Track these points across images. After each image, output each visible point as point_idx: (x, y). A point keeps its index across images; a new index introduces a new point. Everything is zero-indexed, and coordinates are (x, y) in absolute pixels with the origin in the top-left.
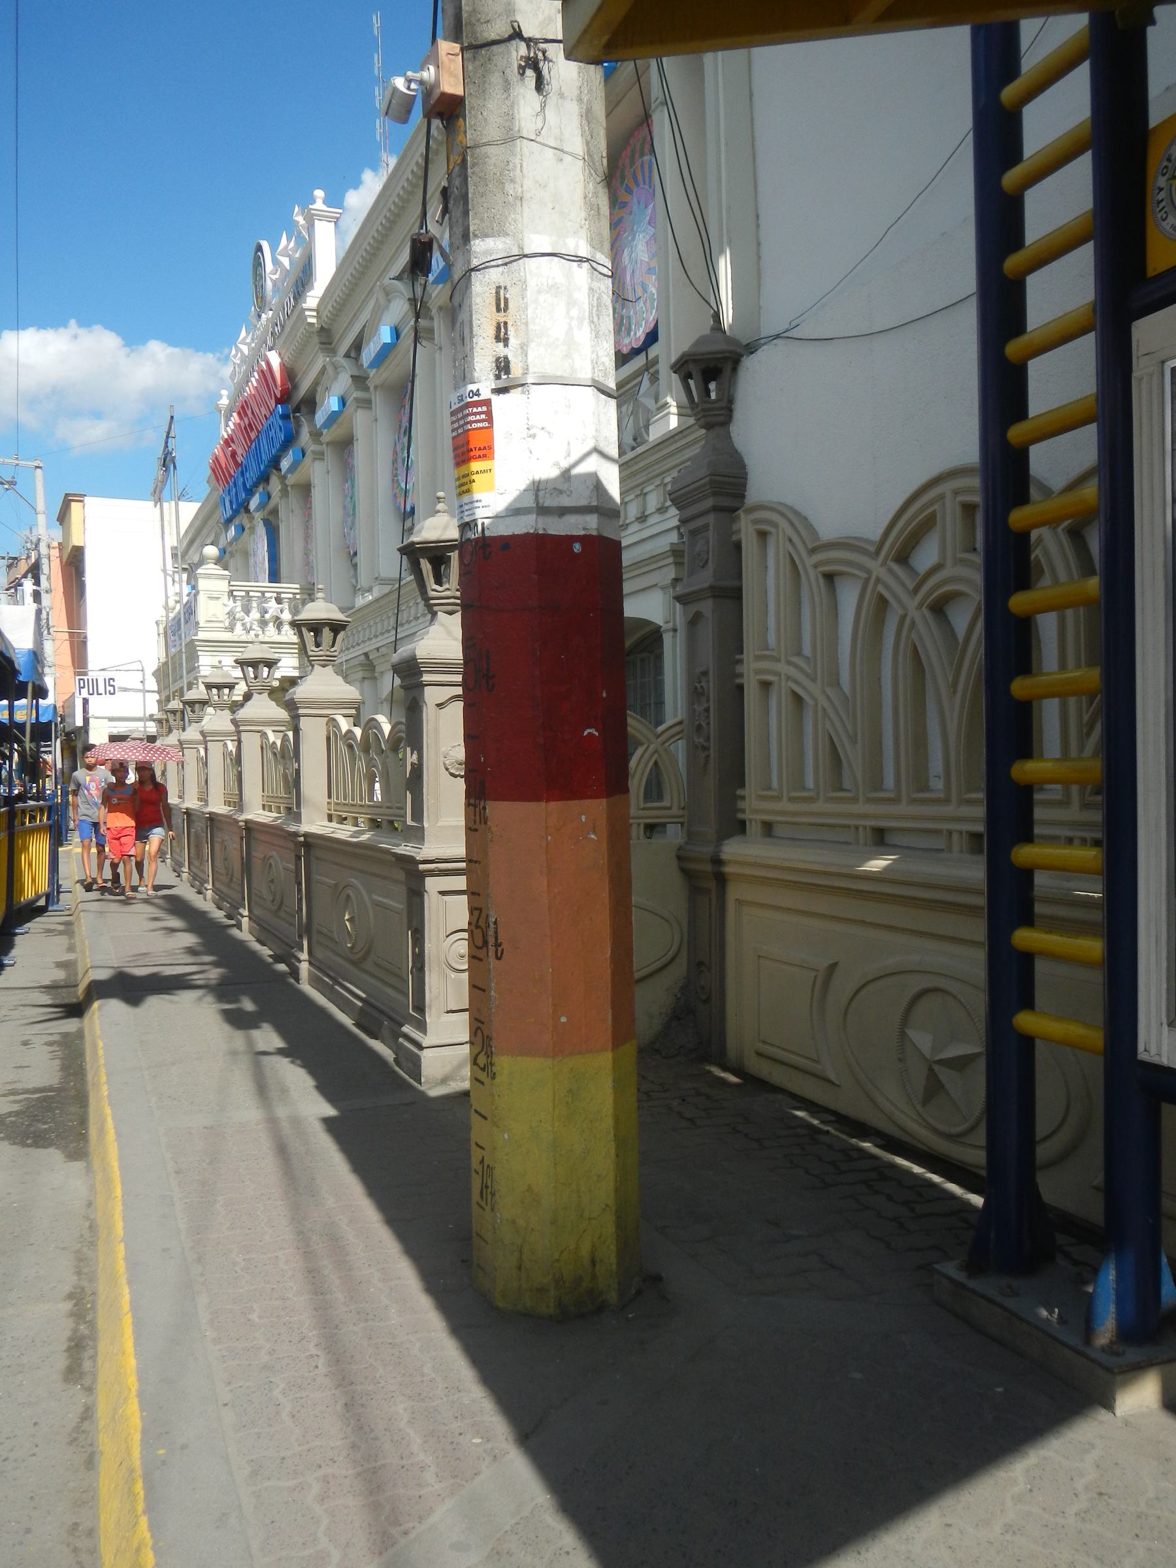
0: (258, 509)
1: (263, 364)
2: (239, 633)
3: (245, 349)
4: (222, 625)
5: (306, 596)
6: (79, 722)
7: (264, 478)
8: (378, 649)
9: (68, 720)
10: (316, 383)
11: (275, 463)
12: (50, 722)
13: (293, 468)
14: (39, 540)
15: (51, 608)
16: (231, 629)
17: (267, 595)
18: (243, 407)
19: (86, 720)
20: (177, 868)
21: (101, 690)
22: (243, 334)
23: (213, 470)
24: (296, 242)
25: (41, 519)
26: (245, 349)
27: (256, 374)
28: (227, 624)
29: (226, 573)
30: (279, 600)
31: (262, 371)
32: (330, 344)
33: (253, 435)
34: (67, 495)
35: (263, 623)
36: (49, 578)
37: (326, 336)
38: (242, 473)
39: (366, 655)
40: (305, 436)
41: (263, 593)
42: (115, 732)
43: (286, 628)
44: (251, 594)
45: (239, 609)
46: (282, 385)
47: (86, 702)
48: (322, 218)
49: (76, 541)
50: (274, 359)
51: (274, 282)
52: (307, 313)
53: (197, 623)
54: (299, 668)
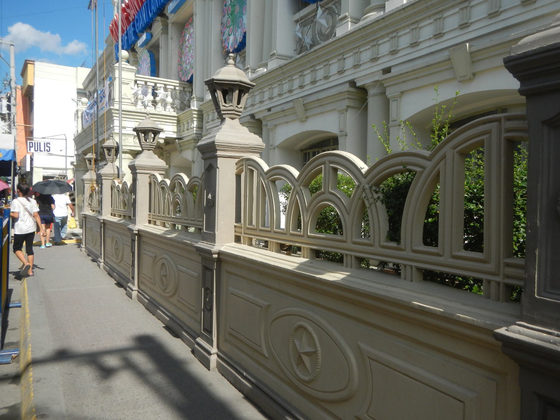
0: (142, 46)
2: (140, 107)
4: (129, 101)
5: (182, 89)
6: (28, 169)
7: (148, 26)
8: (269, 110)
9: (22, 169)
11: (161, 12)
12: (10, 161)
13: (174, 11)
14: (11, 79)
15: (16, 114)
16: (135, 104)
17: (158, 85)
19: (32, 168)
20: (122, 282)
21: (42, 149)
23: (112, 31)
25: (13, 70)
28: (133, 100)
29: (134, 68)
30: (166, 89)
34: (26, 60)
35: (154, 103)
36: (15, 99)
38: (134, 26)
41: (156, 84)
42: (46, 174)
43: (169, 107)
45: (140, 92)
47: (32, 160)
49: (30, 83)
54: (177, 132)
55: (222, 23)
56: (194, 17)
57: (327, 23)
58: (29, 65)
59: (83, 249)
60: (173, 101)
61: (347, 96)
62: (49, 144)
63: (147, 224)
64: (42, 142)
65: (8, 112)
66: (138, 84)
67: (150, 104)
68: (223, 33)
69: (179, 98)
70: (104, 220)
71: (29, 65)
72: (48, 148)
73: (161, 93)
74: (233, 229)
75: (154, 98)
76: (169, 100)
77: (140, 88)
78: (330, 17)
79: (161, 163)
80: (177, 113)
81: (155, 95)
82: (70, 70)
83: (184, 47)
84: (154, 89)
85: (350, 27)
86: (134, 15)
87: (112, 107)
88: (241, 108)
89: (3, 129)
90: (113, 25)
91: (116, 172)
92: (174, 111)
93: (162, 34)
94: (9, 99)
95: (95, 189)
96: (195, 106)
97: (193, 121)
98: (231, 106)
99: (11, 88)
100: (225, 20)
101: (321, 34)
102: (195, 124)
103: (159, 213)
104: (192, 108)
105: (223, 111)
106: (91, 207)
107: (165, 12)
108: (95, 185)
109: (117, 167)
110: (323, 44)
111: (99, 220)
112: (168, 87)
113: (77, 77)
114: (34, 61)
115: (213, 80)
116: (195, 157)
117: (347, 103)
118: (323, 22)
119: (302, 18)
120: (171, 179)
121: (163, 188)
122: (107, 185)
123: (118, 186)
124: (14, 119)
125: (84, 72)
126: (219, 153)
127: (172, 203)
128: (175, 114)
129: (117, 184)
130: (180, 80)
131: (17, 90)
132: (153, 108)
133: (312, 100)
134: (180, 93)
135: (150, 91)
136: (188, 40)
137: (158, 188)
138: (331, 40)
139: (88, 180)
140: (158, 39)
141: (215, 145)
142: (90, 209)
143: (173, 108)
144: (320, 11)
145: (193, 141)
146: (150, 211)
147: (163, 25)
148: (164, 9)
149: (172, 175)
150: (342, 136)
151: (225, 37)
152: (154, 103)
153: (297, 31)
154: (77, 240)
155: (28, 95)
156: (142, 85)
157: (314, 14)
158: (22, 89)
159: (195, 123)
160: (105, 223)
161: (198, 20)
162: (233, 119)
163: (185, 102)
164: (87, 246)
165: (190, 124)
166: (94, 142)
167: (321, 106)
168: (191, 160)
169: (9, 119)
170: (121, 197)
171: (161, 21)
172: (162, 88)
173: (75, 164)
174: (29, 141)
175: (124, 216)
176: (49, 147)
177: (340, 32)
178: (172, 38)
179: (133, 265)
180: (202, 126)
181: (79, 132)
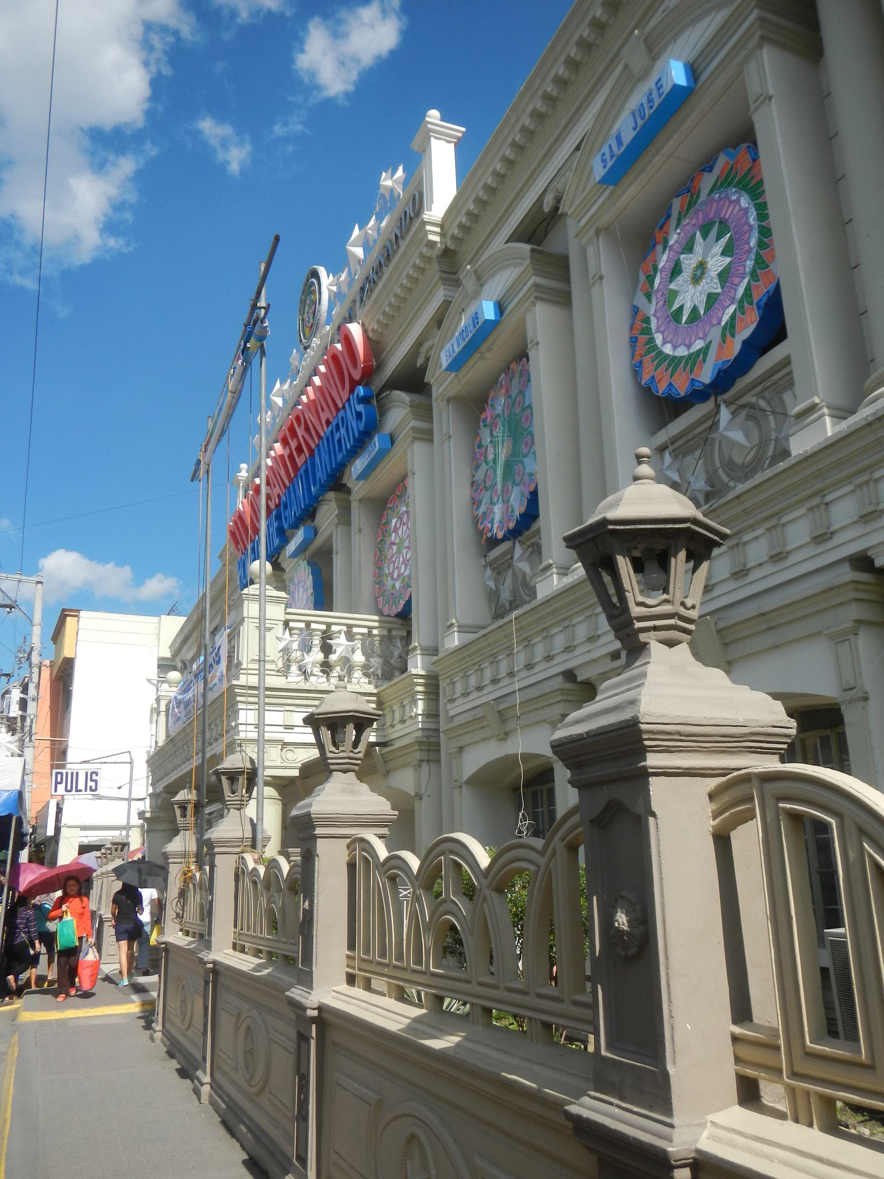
0: (294, 555)
1: (339, 346)
2: (294, 679)
3: (279, 401)
5: (386, 633)
6: (50, 832)
7: (309, 514)
9: (39, 831)
10: (419, 344)
11: (336, 483)
12: (10, 816)
13: (364, 475)
14: (32, 648)
16: (285, 672)
17: (334, 628)
18: (292, 430)
19: (58, 830)
21: (81, 786)
22: (278, 386)
23: (233, 534)
24: (377, 219)
25: (37, 630)
26: (279, 401)
27: (322, 368)
28: (280, 665)
29: (282, 594)
30: (350, 636)
31: (335, 357)
32: (455, 273)
33: (300, 461)
37: (449, 260)
39: (569, 675)
40: (399, 411)
41: (329, 625)
42: (86, 841)
43: (357, 674)
44: (313, 626)
45: (295, 646)
46: (364, 362)
47: (59, 811)
48: (441, 136)
49: (67, 653)
50: (355, 330)
51: (335, 298)
52: (428, 228)
53: (239, 664)
55: (473, 483)
56: (409, 481)
57: (748, 436)
58: (68, 618)
59: (158, 1035)
60: (367, 660)
61: (853, 595)
62: (97, 774)
63: (344, 987)
64: (82, 770)
65: (21, 713)
66: (291, 629)
67: (317, 670)
68: (476, 503)
69: (378, 652)
70: (214, 963)
71: (68, 618)
72: (93, 784)
73: (340, 643)
74: (727, 1050)
75: (326, 657)
76: (359, 658)
77: (295, 637)
78: (751, 424)
79: (380, 805)
80: (376, 687)
81: (327, 649)
82: (145, 624)
83: (386, 546)
84: (327, 636)
85: (830, 428)
86: (279, 496)
87: (234, 682)
88: (693, 607)
89: (8, 749)
90: (235, 522)
91: (248, 834)
92: (370, 683)
93: (337, 525)
94: (25, 689)
95: (193, 878)
96: (417, 666)
97: (414, 702)
98: (667, 601)
99: (30, 664)
100: (480, 475)
101: (730, 466)
102: (420, 707)
103: (383, 954)
104: (414, 671)
105: (641, 619)
106: (181, 923)
107: (345, 480)
108: (193, 867)
109: (251, 820)
110: (741, 488)
111: (202, 962)
112: (355, 630)
113: (159, 635)
114: (78, 611)
115: (604, 522)
116: (423, 784)
117: (854, 612)
118: (738, 436)
119: (674, 440)
120: (423, 853)
121: (393, 879)
122: (225, 866)
123: (254, 869)
124: (31, 726)
125: (173, 625)
126: (653, 760)
127: (428, 927)
128: (371, 689)
129: (251, 865)
130: (380, 613)
131: (43, 668)
132: (324, 679)
133: (742, 618)
134: (381, 642)
135: (317, 641)
136: (396, 530)
137: (378, 879)
138: (759, 478)
139: (176, 855)
140: (330, 537)
141: (640, 732)
142: (178, 927)
143: (366, 675)
144: (725, 414)
145: (417, 747)
146: (351, 946)
147: (339, 507)
148: (342, 475)
149: (426, 837)
150: (852, 701)
151: (483, 508)
152: (326, 667)
153: (667, 468)
154: (144, 1004)
155: (63, 676)
156: (300, 629)
157: (710, 423)
158: (51, 666)
159: (421, 705)
160: (217, 971)
161: (417, 488)
162: (671, 644)
163: (393, 661)
164: (168, 1026)
165: (407, 708)
166: (195, 761)
167: (770, 629)
168: (413, 794)
169: (23, 727)
170: (263, 901)
171: (336, 499)
172: (343, 635)
173: (148, 815)
174: (54, 771)
175: (270, 954)
176: (96, 781)
177: (801, 444)
178: (360, 531)
179: (303, 1117)
180: (437, 710)
181: (160, 744)
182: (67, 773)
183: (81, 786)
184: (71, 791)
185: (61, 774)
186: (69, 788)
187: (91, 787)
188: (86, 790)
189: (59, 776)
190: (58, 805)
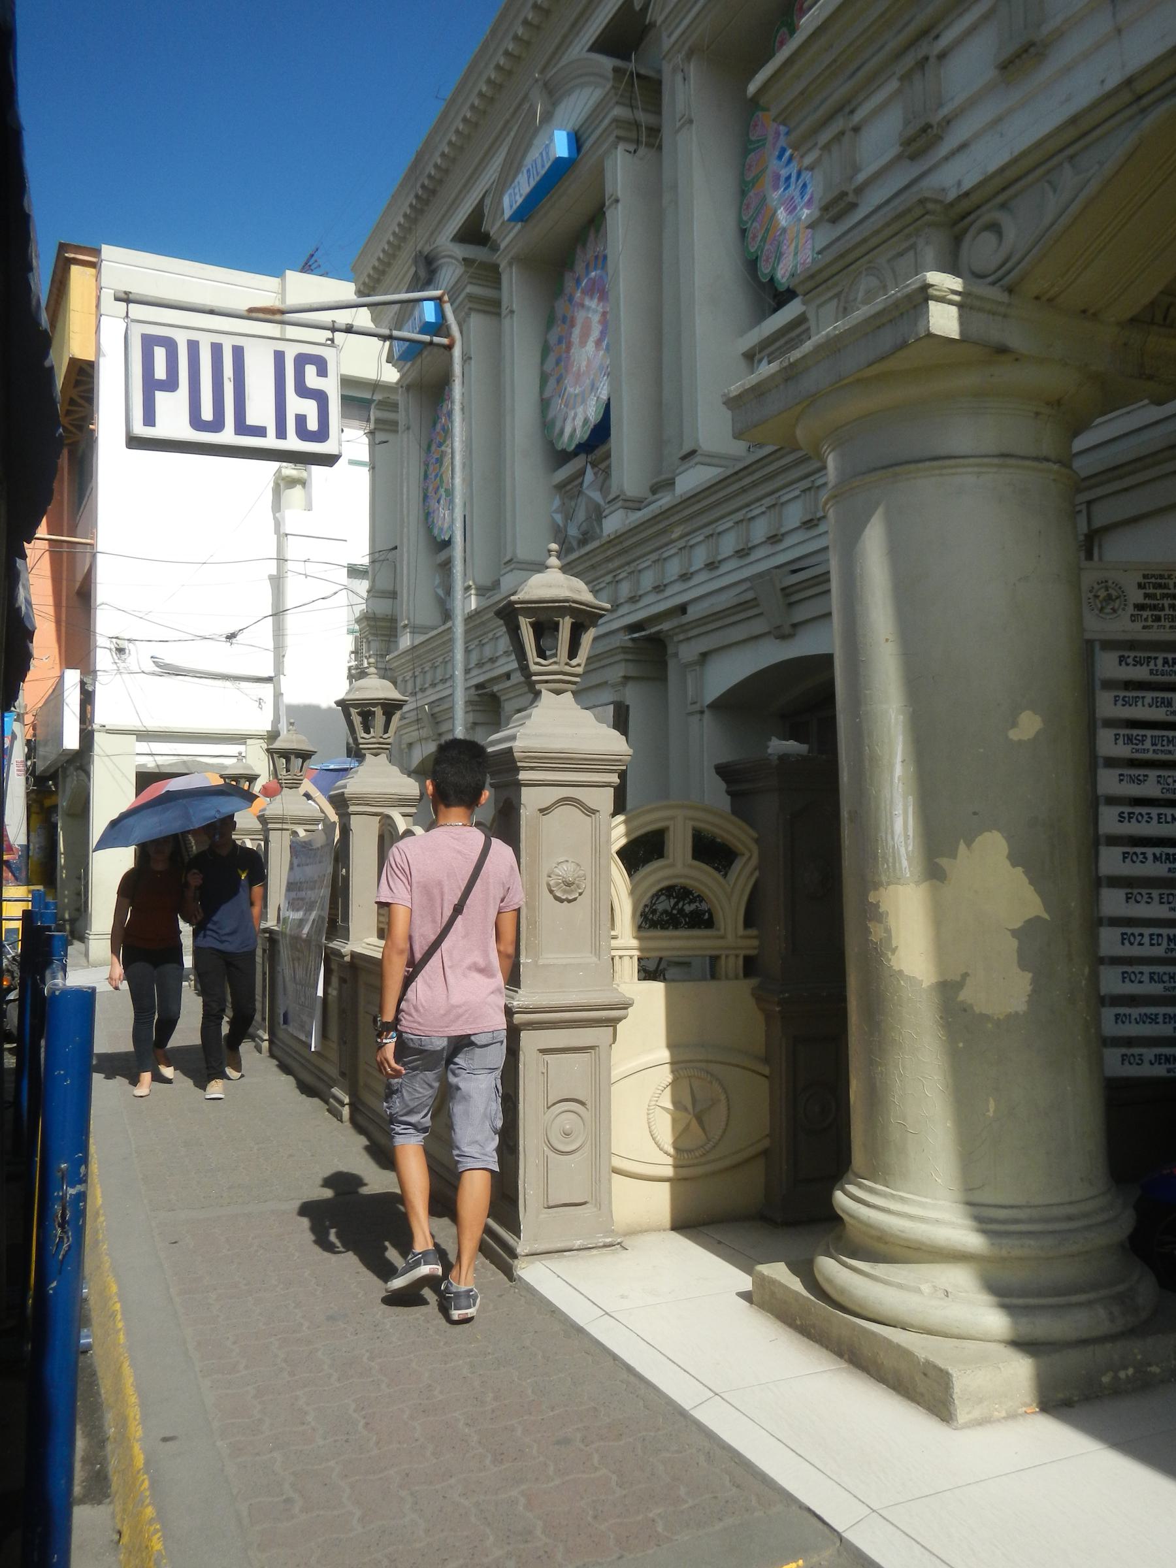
6: (71, 741)
19: (87, 736)
21: (261, 411)
42: (150, 764)
47: (87, 698)
62: (322, 372)
72: (309, 408)
176: (321, 398)
182: (193, 347)
183: (261, 411)
184: (217, 425)
185: (170, 346)
186: (207, 414)
187: (301, 420)
188: (281, 433)
189: (160, 354)
190: (83, 684)
